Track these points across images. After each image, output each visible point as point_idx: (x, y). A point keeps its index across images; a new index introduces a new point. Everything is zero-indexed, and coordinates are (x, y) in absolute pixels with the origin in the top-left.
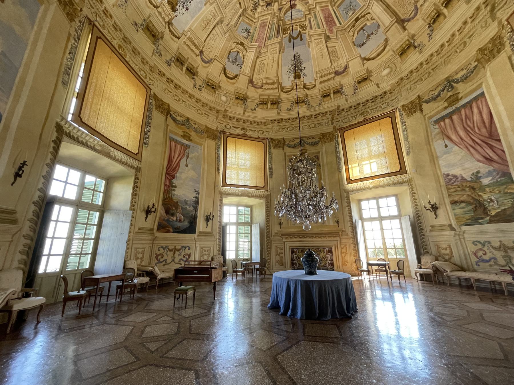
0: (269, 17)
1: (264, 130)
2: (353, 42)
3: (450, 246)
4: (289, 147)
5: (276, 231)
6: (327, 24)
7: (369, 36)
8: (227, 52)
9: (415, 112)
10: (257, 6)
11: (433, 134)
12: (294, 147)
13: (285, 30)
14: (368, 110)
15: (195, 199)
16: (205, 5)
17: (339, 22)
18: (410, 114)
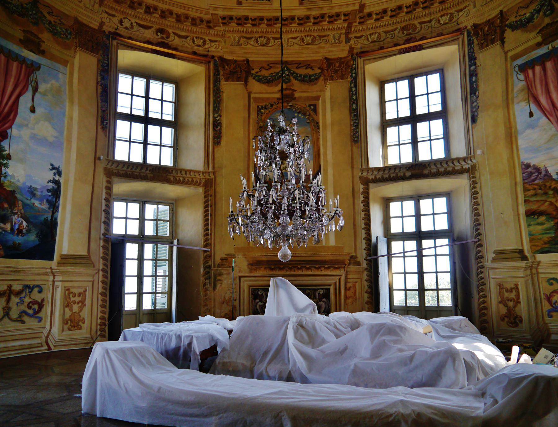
1: (207, 38)
3: (516, 287)
4: (259, 81)
5: (224, 256)
9: (492, 43)
11: (515, 90)
12: (268, 81)
14: (416, 22)
15: (51, 185)
18: (485, 44)
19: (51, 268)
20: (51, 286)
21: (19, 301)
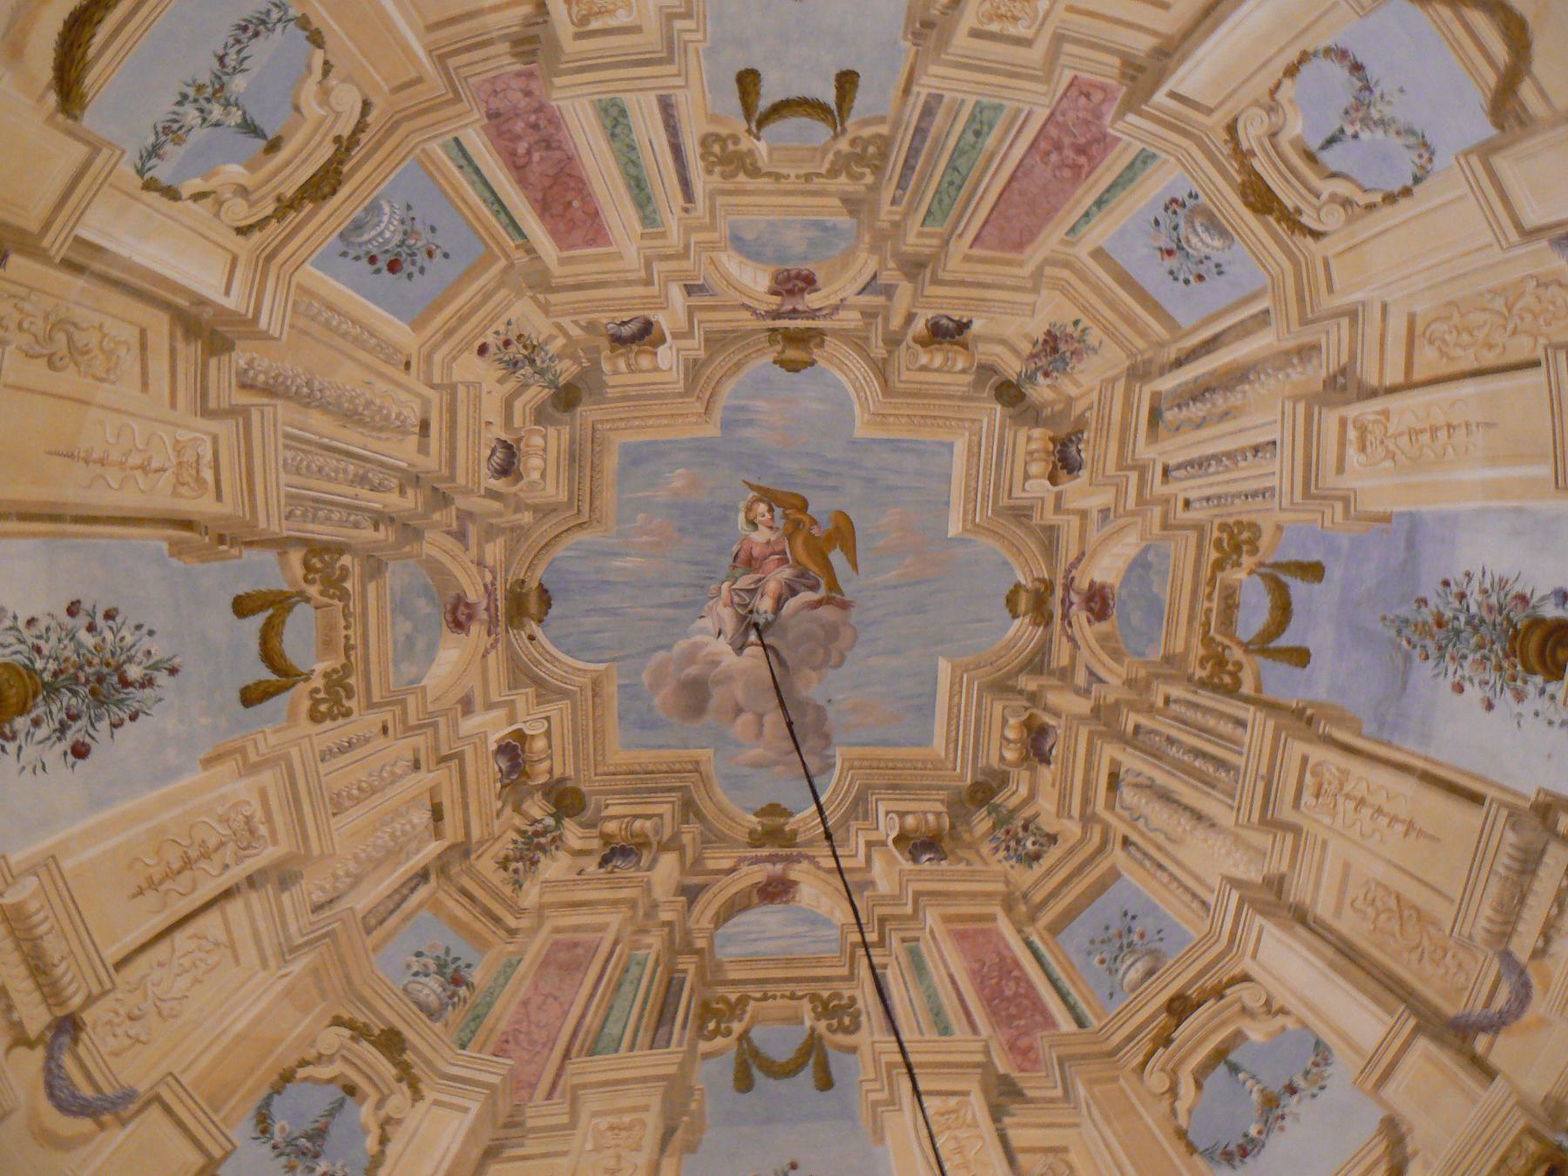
0: (614, 920)
2: (1181, 1134)
6: (992, 1012)
7: (1270, 1103)
8: (267, 1072)
10: (541, 847)
13: (718, 1015)
16: (208, 762)
17: (1071, 1008)
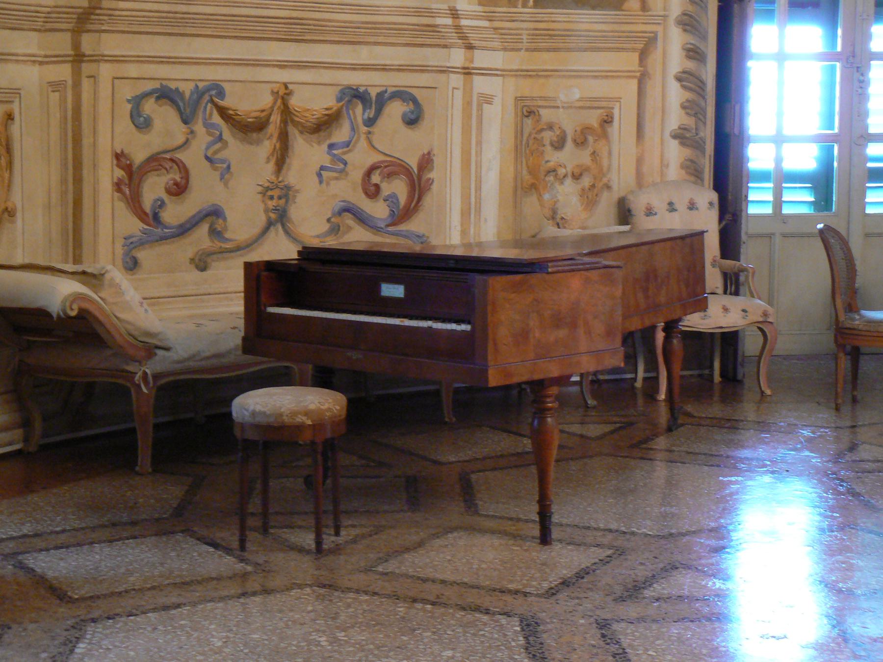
19: (454, 14)
20: (459, 94)
21: (327, 161)
